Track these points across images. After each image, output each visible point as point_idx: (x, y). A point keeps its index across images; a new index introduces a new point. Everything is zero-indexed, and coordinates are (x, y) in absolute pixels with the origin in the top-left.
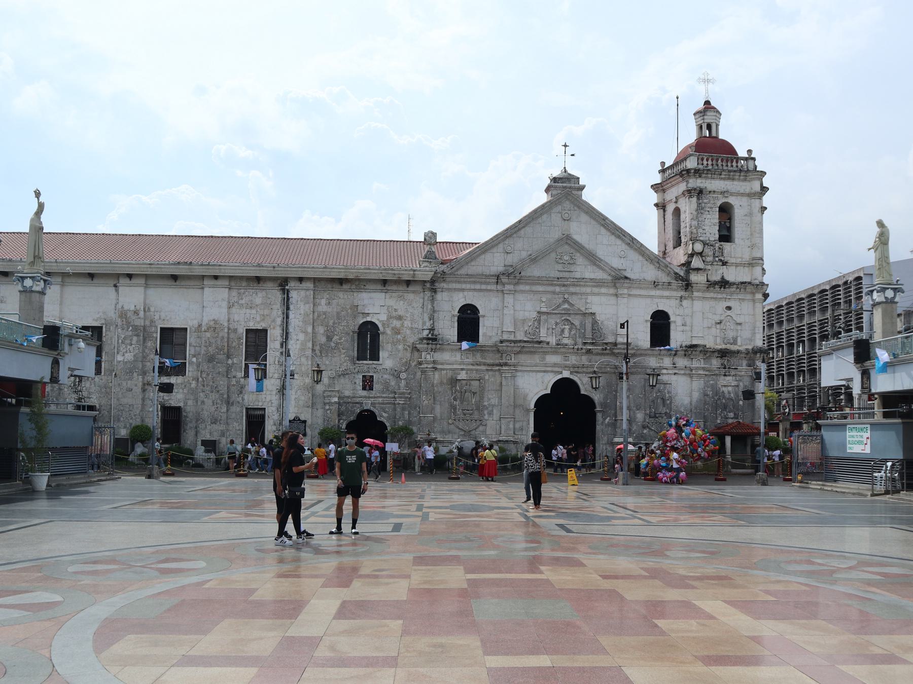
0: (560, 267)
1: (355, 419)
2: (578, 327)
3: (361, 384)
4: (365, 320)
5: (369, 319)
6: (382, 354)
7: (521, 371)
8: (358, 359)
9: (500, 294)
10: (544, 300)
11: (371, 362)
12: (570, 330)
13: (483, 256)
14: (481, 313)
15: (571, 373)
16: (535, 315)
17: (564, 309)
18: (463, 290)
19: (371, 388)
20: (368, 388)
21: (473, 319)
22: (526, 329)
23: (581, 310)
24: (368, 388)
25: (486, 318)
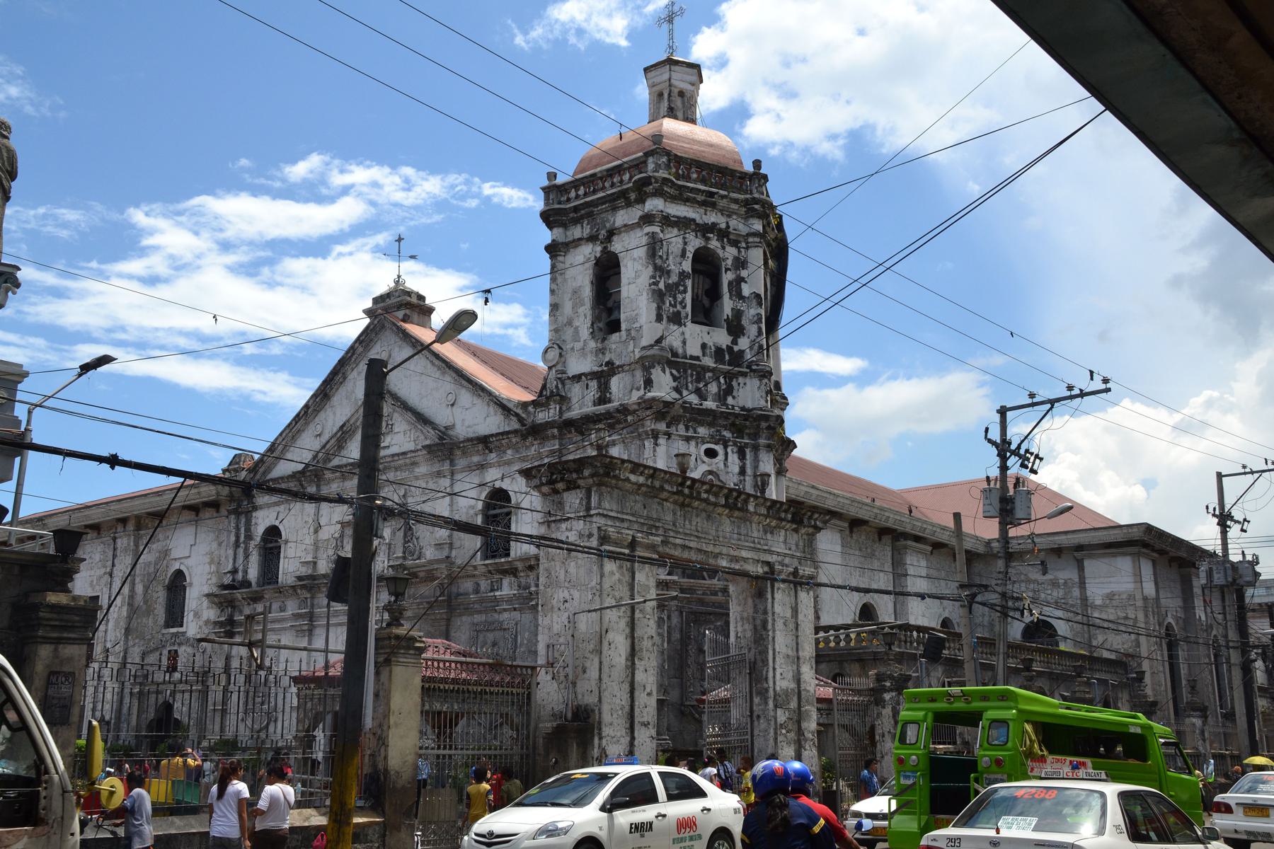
6: (189, 617)
25: (289, 544)
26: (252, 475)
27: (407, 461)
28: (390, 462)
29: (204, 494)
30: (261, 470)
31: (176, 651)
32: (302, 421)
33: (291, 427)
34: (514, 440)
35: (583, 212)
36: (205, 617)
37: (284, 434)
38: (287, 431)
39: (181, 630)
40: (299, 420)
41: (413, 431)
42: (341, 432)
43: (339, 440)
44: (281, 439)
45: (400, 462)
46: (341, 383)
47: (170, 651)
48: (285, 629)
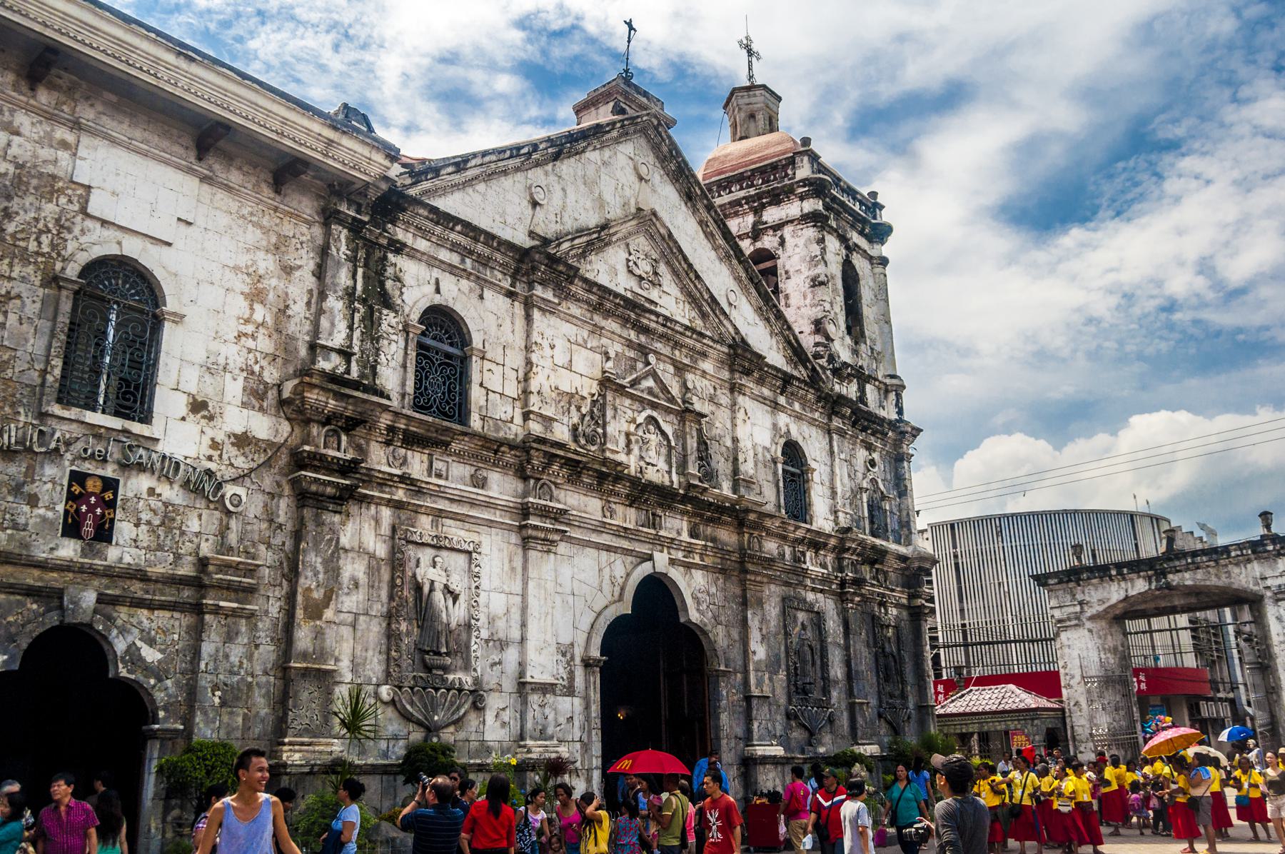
0: (632, 284)
1: (16, 666)
2: (673, 444)
3: (60, 508)
4: (113, 250)
5: (132, 248)
7: (570, 540)
8: (64, 398)
9: (519, 309)
10: (612, 355)
11: (116, 423)
12: (660, 445)
13: (481, 187)
14: (477, 341)
15: (672, 562)
16: (595, 388)
17: (650, 391)
18: (432, 262)
19: (104, 534)
20: (88, 528)
21: (448, 356)
22: (576, 420)
23: (676, 403)
24: (88, 528)
26: (409, 181)
27: (698, 345)
28: (677, 332)
29: (342, 154)
30: (426, 185)
31: (111, 485)
32: (515, 162)
33: (502, 156)
34: (809, 396)
35: (835, 206)
36: (237, 419)
37: (487, 159)
38: (493, 158)
39: (136, 428)
40: (518, 155)
41: (687, 306)
42: (595, 236)
43: (590, 243)
44: (478, 161)
45: (688, 340)
46: (577, 154)
47: (78, 478)
48: (490, 524)
